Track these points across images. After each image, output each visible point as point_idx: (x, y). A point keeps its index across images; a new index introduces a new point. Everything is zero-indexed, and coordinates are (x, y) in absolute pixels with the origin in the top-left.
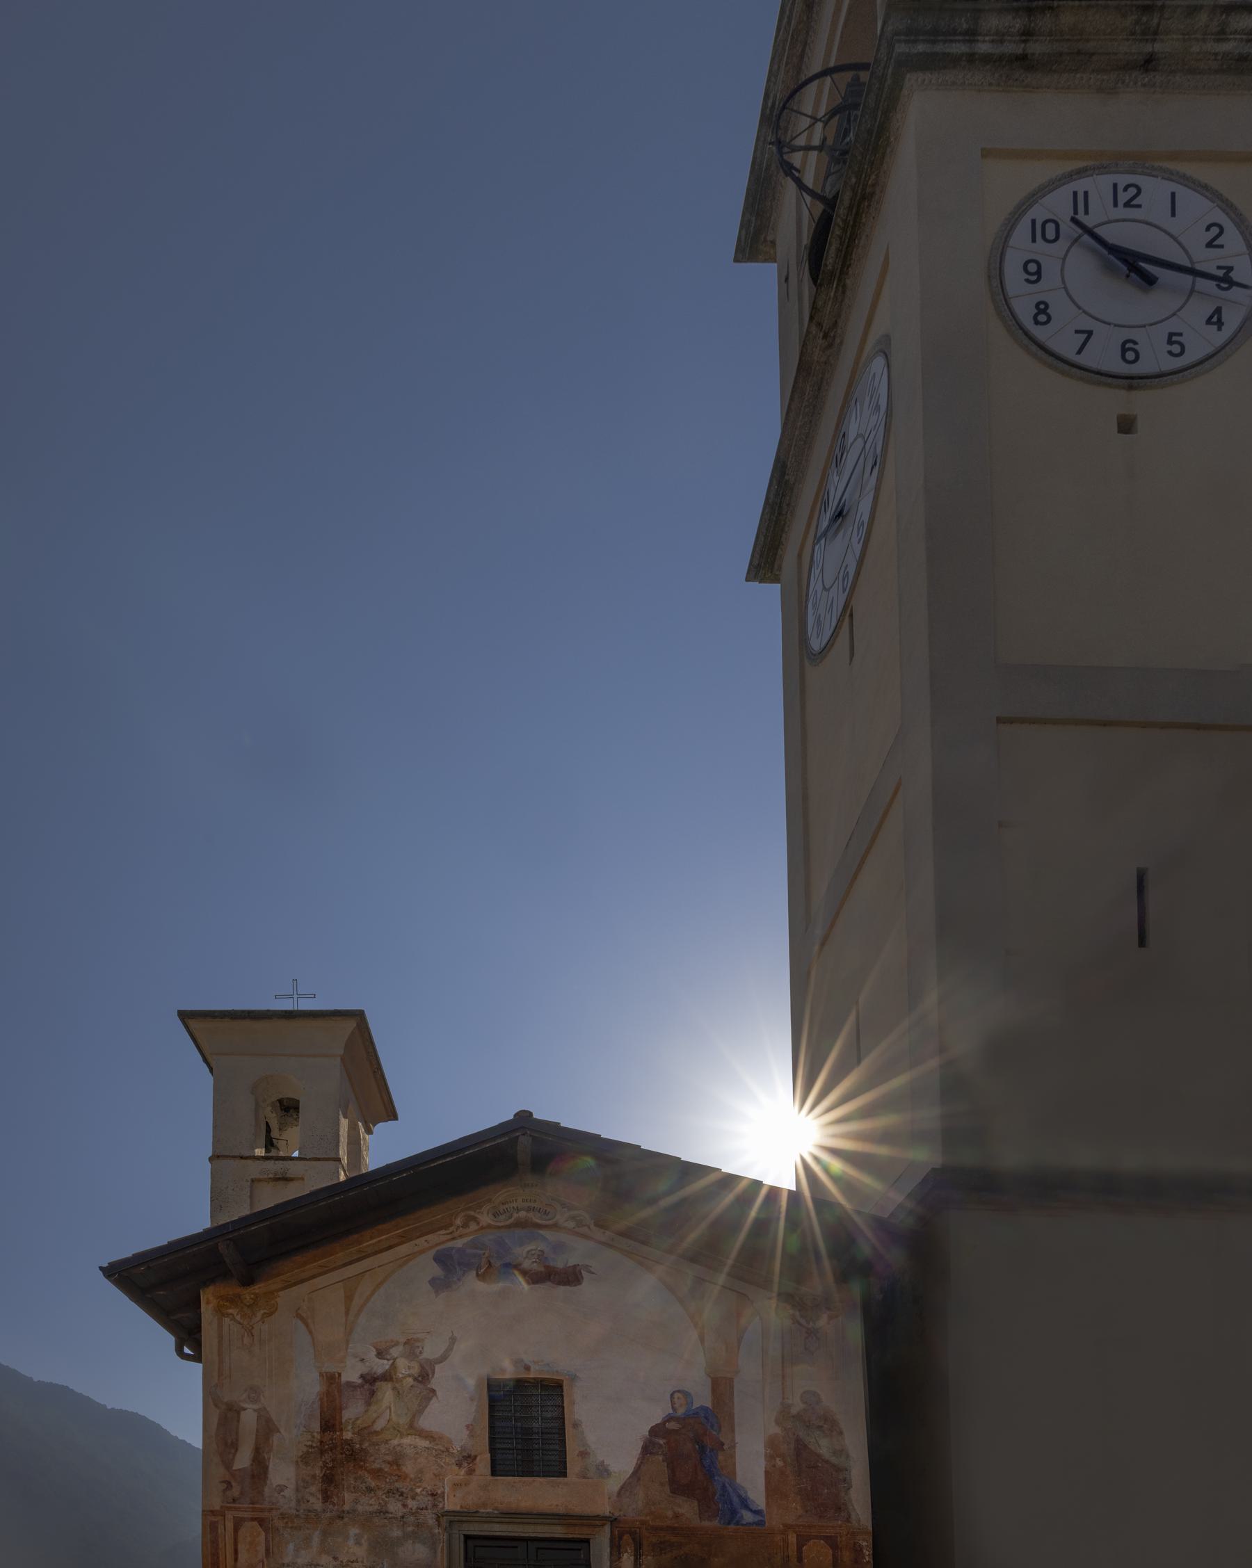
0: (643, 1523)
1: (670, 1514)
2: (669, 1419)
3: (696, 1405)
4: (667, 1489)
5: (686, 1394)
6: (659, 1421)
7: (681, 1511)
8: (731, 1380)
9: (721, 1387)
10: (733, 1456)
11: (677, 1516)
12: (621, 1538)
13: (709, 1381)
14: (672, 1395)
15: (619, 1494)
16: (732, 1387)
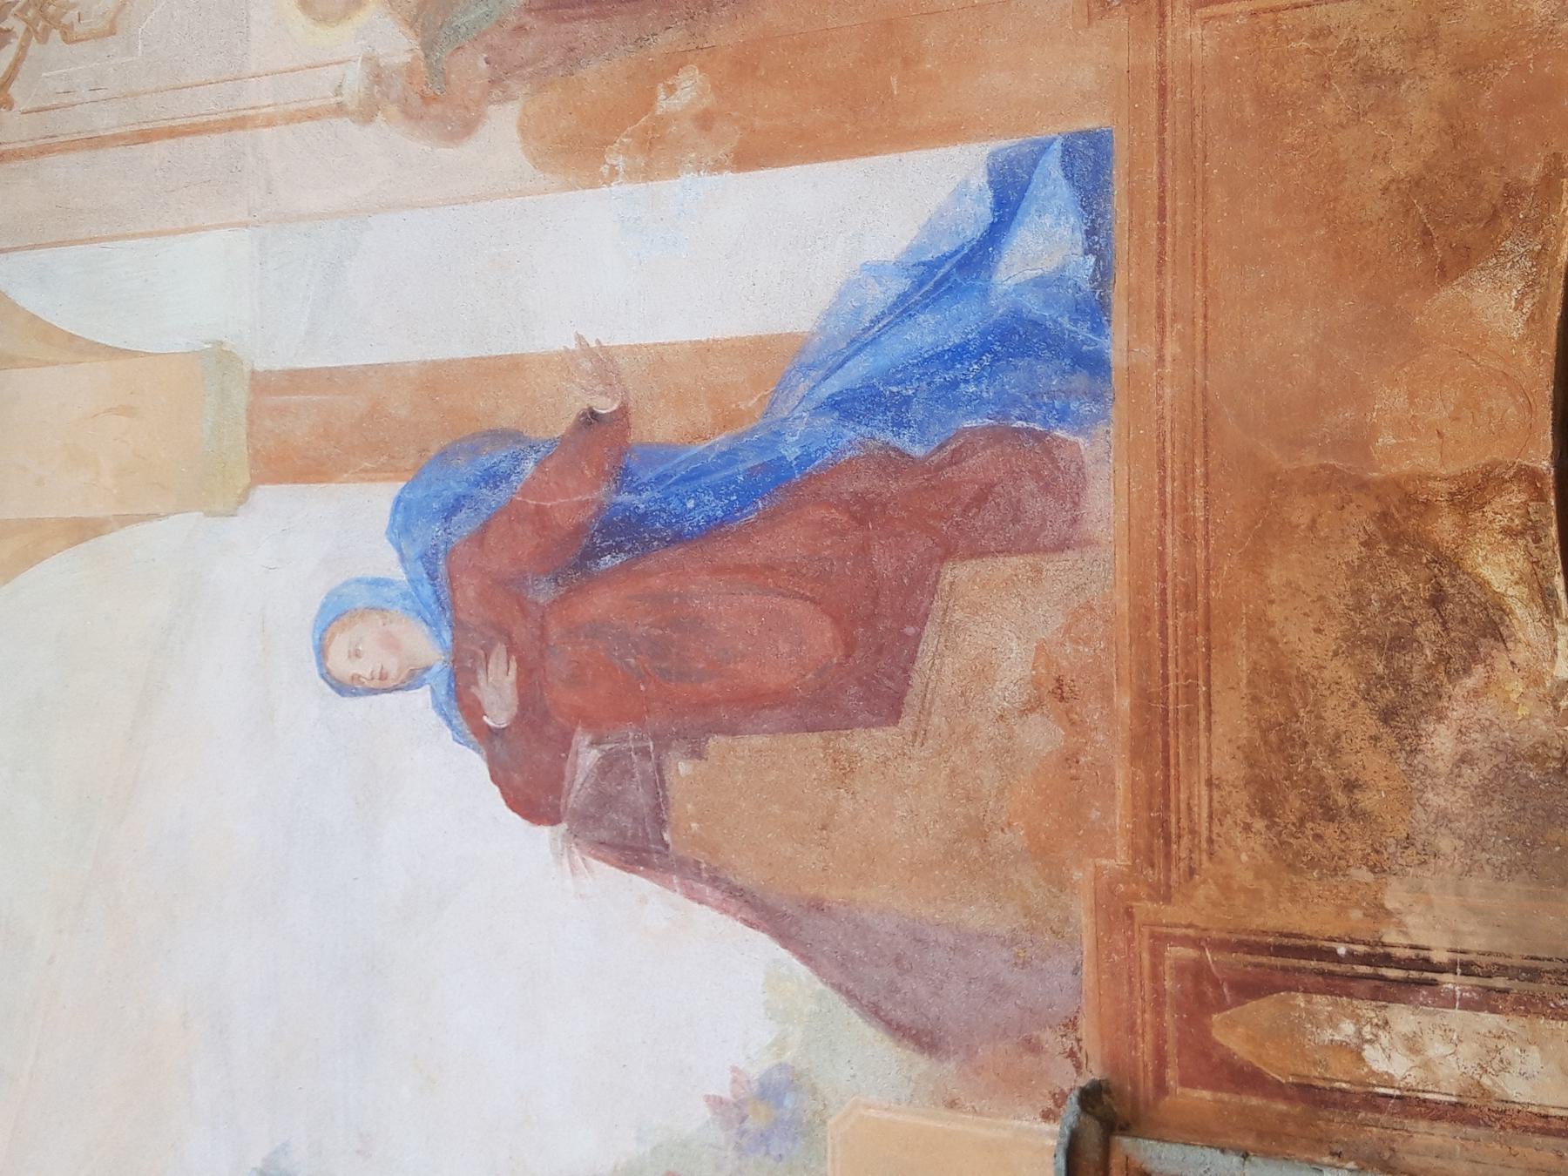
0: (1115, 911)
1: (1041, 736)
2: (462, 703)
3: (386, 562)
4: (868, 743)
5: (335, 616)
6: (475, 764)
7: (1015, 666)
8: (262, 384)
9: (298, 431)
10: (659, 359)
11: (1057, 692)
12: (1246, 1078)
13: (269, 496)
14: (344, 688)
15: (922, 1038)
16: (296, 379)
